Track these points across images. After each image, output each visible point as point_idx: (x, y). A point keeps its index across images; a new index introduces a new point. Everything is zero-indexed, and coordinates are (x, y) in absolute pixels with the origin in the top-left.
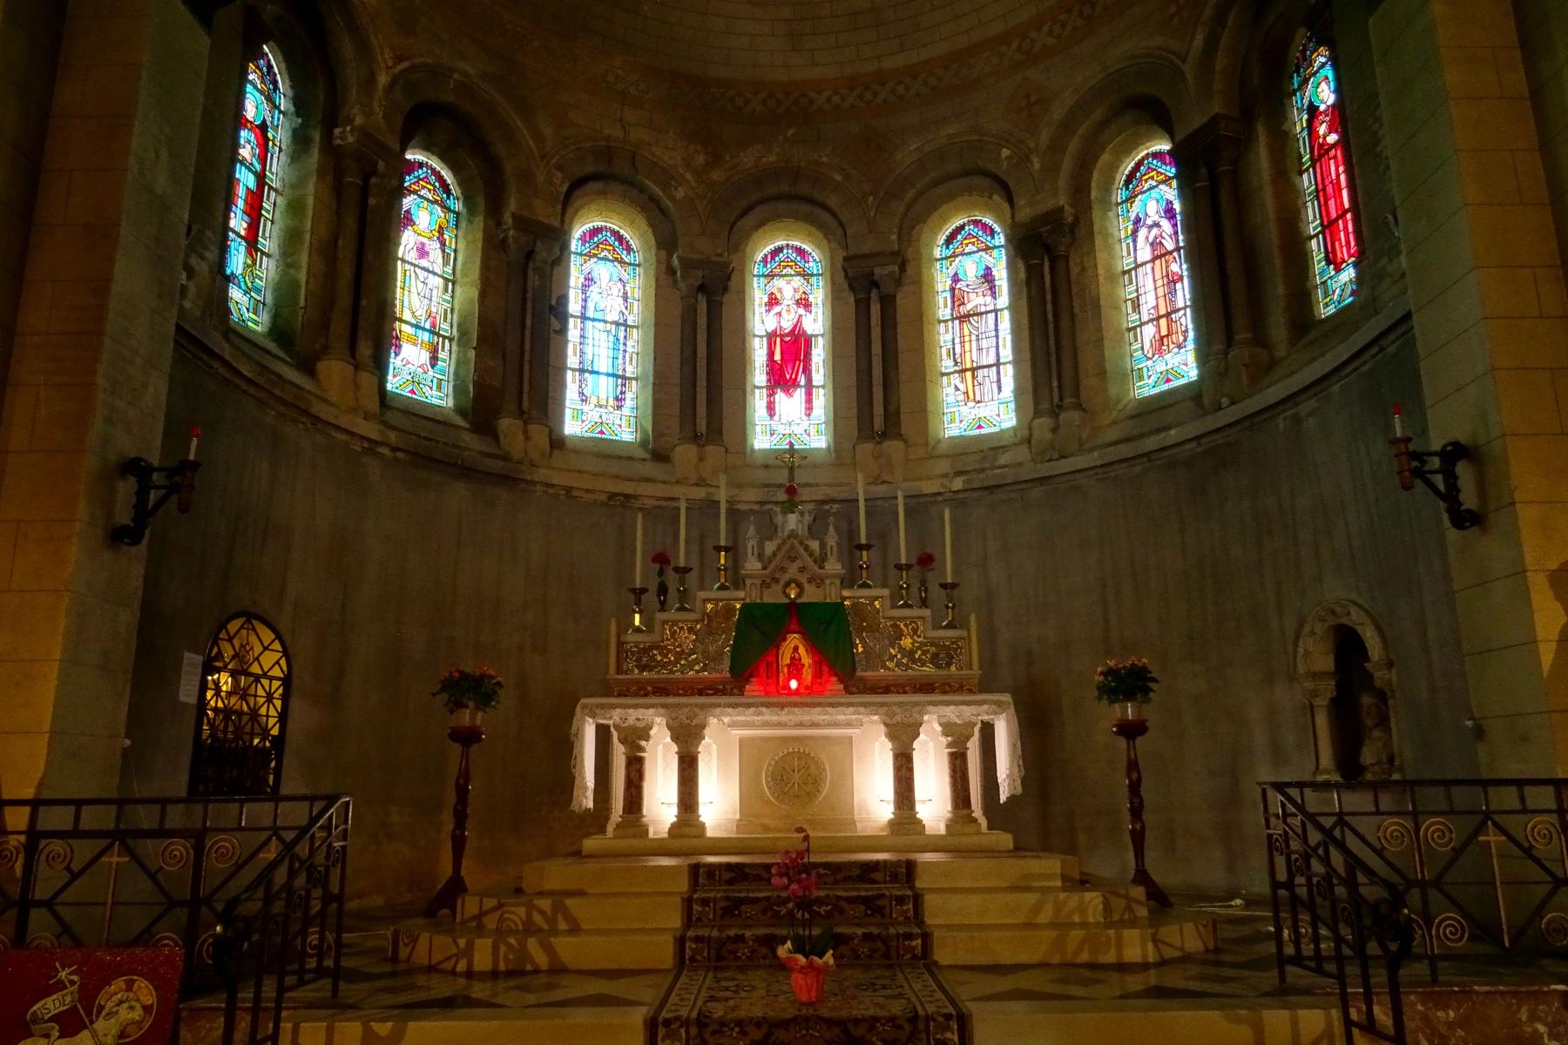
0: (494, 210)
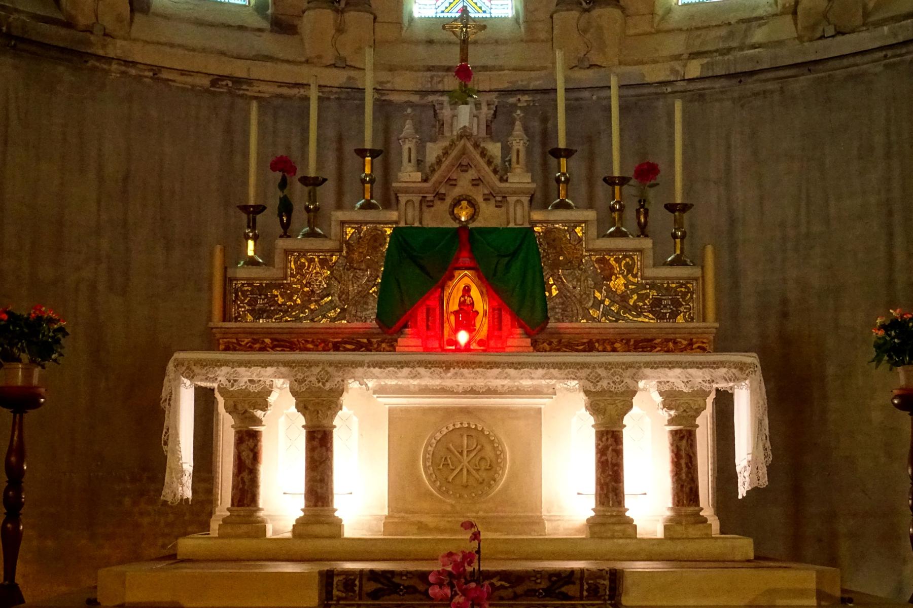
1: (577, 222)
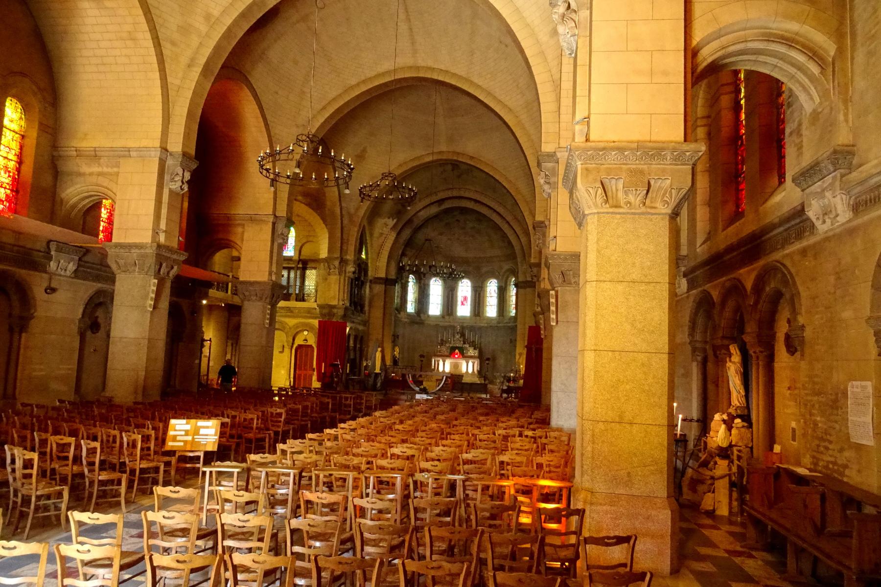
0: (420, 283)
1: (467, 346)
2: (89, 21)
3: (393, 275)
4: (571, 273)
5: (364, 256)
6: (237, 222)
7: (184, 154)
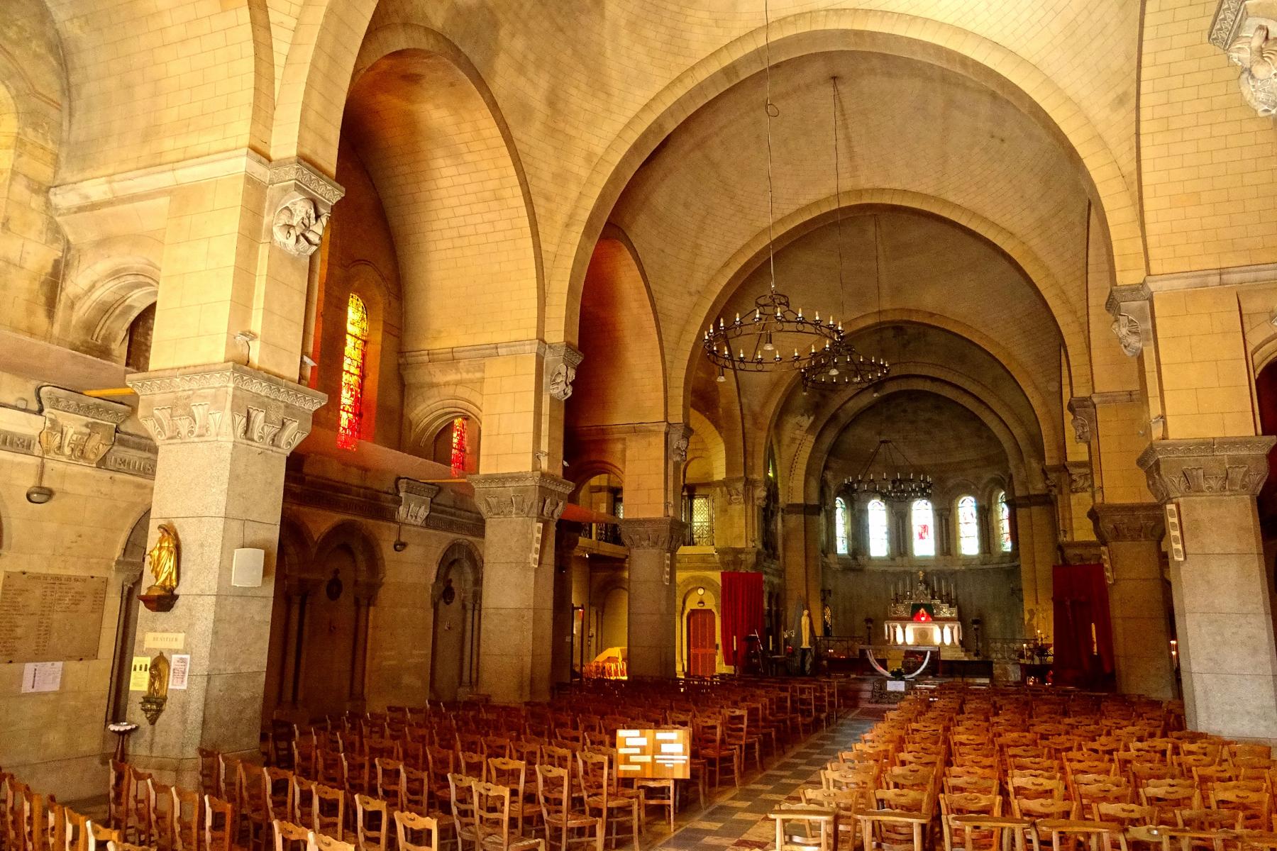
1: (938, 602)
2: (443, 183)
3: (814, 500)
4: (1201, 472)
5: (771, 475)
6: (616, 436)
7: (569, 345)
